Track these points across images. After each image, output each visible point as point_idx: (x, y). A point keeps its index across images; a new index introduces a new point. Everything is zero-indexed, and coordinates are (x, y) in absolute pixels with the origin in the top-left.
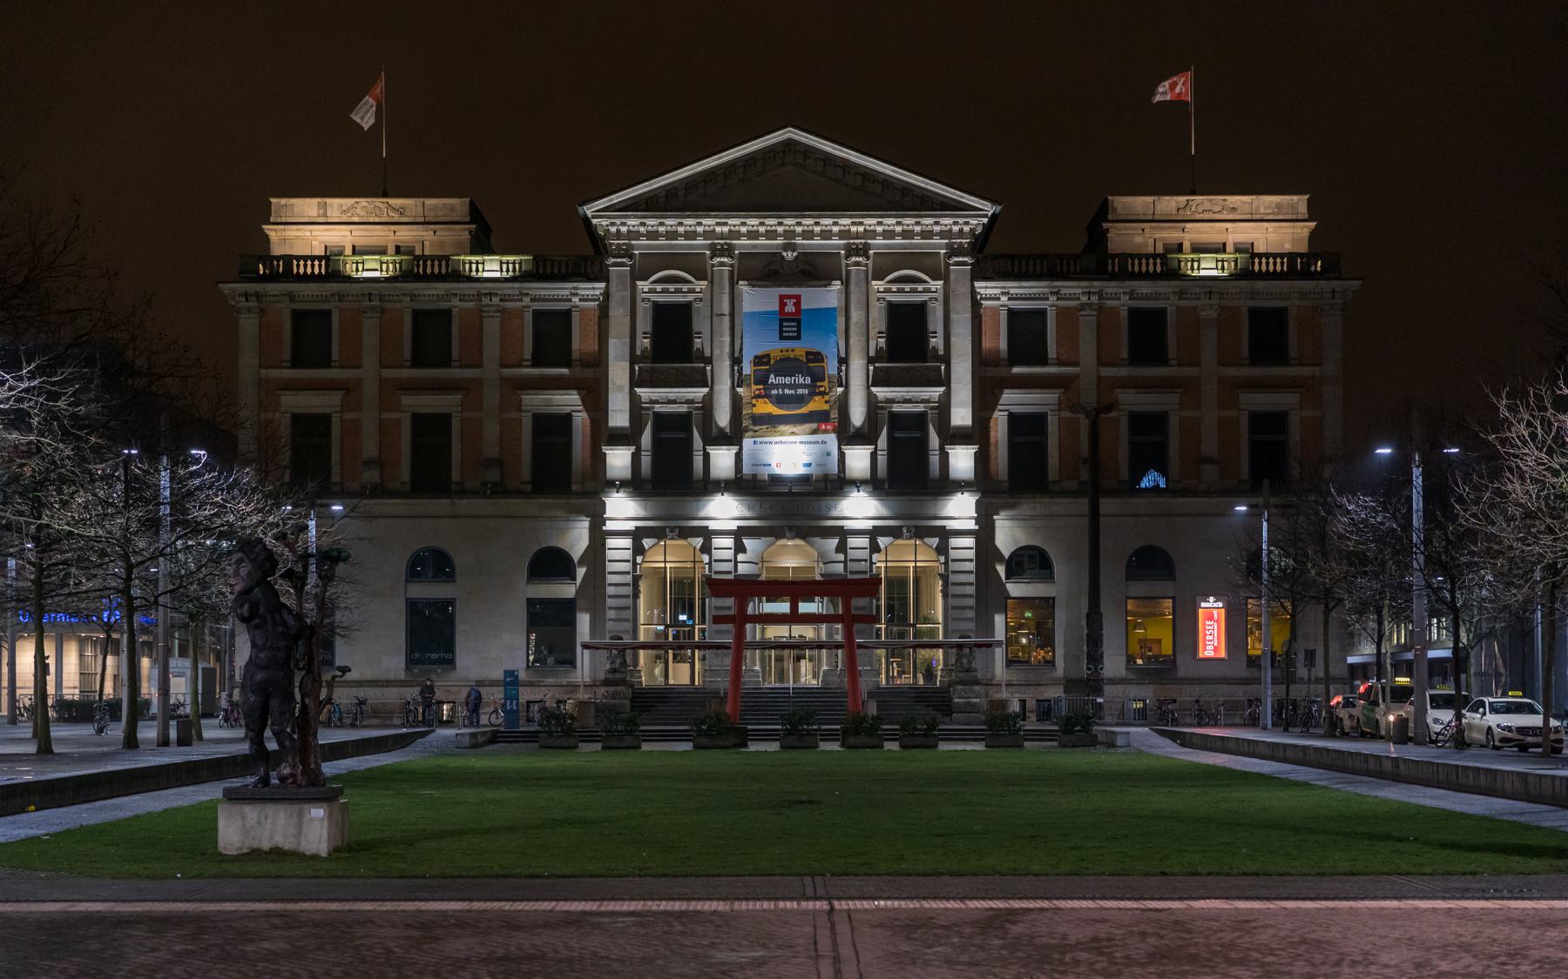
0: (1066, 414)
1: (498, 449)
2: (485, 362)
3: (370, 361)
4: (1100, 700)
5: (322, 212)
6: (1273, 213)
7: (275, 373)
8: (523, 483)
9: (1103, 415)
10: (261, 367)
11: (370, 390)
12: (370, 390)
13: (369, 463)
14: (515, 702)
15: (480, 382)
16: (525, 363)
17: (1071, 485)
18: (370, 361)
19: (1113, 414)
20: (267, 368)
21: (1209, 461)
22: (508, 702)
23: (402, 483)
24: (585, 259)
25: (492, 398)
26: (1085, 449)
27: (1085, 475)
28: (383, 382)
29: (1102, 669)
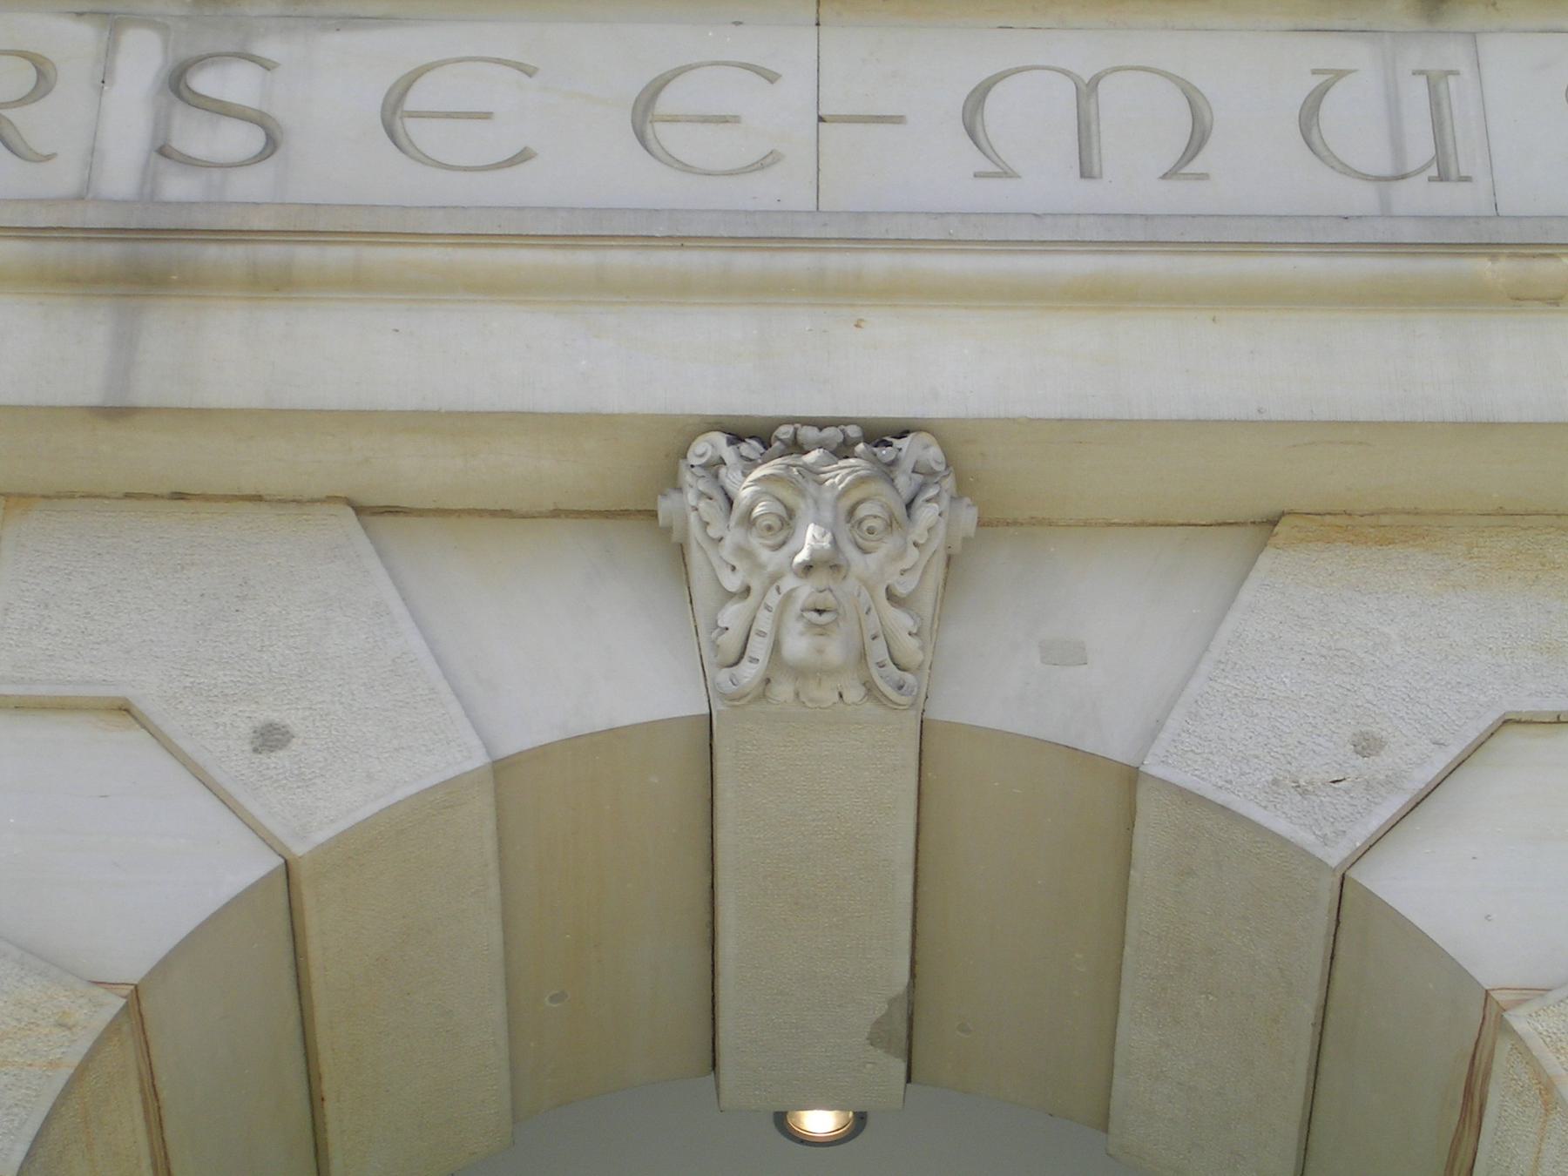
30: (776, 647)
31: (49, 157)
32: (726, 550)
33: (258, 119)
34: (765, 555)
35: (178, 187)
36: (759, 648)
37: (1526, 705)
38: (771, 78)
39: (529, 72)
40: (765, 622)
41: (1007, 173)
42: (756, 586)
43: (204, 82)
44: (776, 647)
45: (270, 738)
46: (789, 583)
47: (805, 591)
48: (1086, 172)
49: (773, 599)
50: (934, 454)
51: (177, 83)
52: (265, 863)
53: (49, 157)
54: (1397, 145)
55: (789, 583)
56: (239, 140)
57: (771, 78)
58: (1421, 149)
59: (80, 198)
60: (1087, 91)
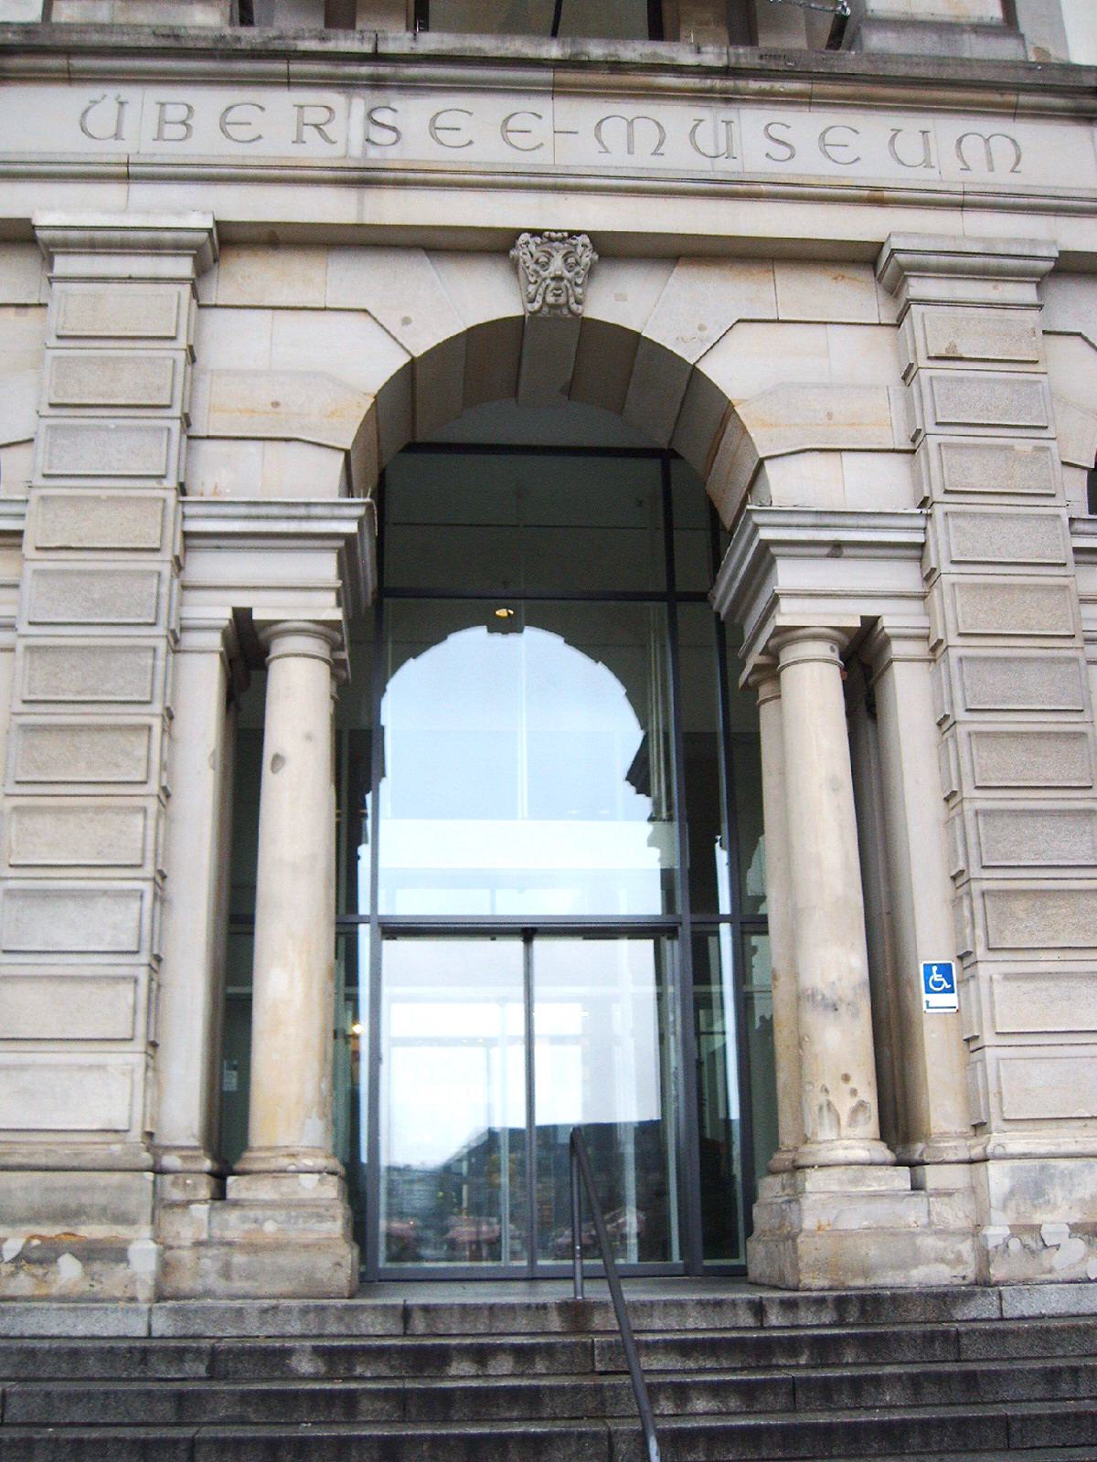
30: (544, 299)
31: (334, 143)
32: (530, 271)
33: (394, 129)
34: (541, 272)
35: (374, 153)
36: (539, 298)
37: (745, 317)
38: (540, 117)
39: (471, 114)
40: (541, 291)
41: (607, 152)
42: (539, 281)
43: (378, 116)
44: (544, 298)
45: (406, 321)
46: (548, 281)
47: (553, 284)
48: (630, 152)
49: (544, 285)
50: (585, 239)
51: (369, 116)
52: (407, 359)
53: (334, 143)
54: (717, 147)
55: (548, 281)
56: (388, 136)
57: (540, 117)
58: (723, 149)
59: (345, 157)
60: (631, 123)
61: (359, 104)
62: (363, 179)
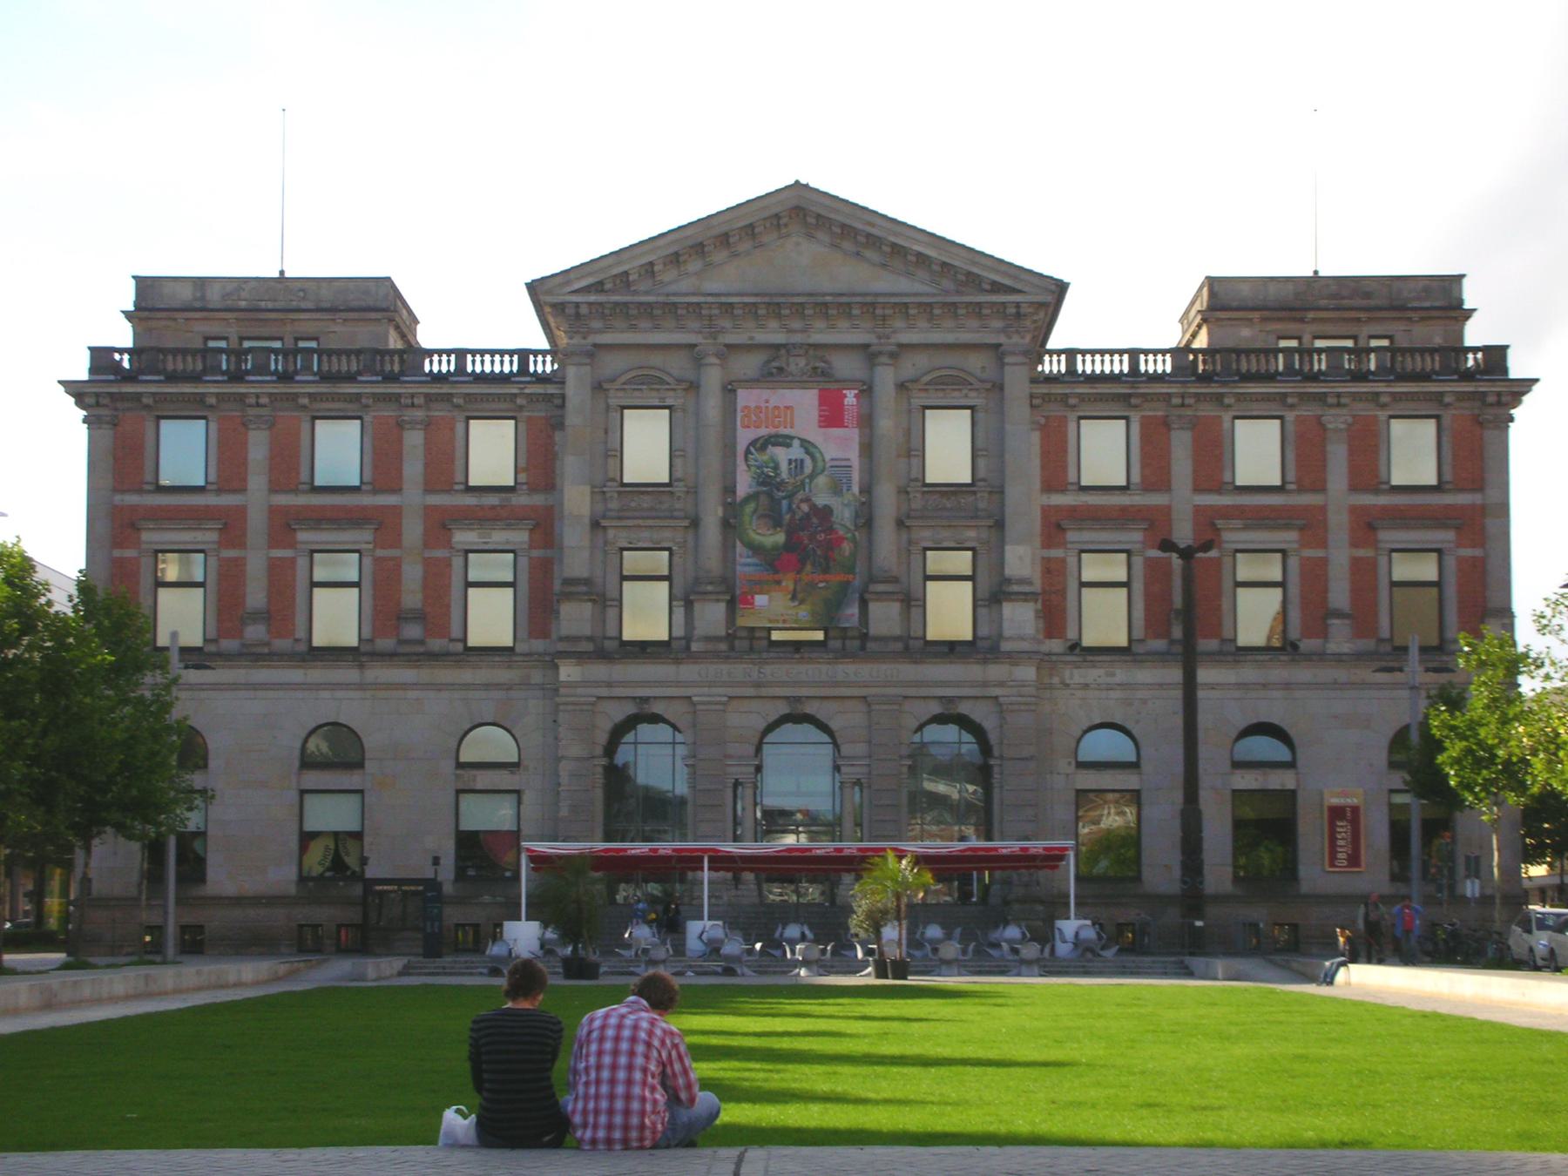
0: (1154, 553)
1: (419, 596)
2: (405, 487)
3: (257, 482)
4: (1199, 923)
5: (198, 295)
6: (1419, 299)
7: (132, 499)
8: (452, 640)
9: (1200, 555)
10: (116, 490)
11: (257, 521)
12: (257, 521)
13: (255, 616)
14: (437, 924)
15: (396, 511)
16: (457, 487)
17: (1159, 644)
18: (257, 482)
19: (1213, 553)
20: (123, 492)
21: (1338, 614)
22: (429, 924)
23: (297, 640)
24: (536, 353)
25: (413, 531)
26: (1178, 601)
27: (1177, 632)
28: (274, 511)
29: (1201, 883)
51: (760, 672)
61: (757, 667)
62: (758, 685)
